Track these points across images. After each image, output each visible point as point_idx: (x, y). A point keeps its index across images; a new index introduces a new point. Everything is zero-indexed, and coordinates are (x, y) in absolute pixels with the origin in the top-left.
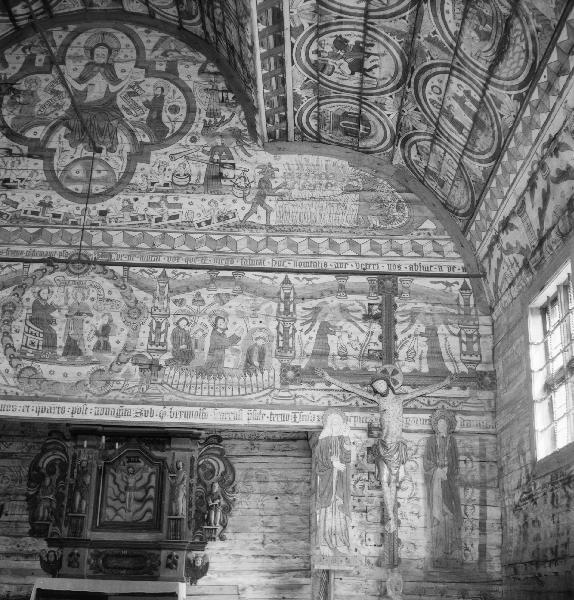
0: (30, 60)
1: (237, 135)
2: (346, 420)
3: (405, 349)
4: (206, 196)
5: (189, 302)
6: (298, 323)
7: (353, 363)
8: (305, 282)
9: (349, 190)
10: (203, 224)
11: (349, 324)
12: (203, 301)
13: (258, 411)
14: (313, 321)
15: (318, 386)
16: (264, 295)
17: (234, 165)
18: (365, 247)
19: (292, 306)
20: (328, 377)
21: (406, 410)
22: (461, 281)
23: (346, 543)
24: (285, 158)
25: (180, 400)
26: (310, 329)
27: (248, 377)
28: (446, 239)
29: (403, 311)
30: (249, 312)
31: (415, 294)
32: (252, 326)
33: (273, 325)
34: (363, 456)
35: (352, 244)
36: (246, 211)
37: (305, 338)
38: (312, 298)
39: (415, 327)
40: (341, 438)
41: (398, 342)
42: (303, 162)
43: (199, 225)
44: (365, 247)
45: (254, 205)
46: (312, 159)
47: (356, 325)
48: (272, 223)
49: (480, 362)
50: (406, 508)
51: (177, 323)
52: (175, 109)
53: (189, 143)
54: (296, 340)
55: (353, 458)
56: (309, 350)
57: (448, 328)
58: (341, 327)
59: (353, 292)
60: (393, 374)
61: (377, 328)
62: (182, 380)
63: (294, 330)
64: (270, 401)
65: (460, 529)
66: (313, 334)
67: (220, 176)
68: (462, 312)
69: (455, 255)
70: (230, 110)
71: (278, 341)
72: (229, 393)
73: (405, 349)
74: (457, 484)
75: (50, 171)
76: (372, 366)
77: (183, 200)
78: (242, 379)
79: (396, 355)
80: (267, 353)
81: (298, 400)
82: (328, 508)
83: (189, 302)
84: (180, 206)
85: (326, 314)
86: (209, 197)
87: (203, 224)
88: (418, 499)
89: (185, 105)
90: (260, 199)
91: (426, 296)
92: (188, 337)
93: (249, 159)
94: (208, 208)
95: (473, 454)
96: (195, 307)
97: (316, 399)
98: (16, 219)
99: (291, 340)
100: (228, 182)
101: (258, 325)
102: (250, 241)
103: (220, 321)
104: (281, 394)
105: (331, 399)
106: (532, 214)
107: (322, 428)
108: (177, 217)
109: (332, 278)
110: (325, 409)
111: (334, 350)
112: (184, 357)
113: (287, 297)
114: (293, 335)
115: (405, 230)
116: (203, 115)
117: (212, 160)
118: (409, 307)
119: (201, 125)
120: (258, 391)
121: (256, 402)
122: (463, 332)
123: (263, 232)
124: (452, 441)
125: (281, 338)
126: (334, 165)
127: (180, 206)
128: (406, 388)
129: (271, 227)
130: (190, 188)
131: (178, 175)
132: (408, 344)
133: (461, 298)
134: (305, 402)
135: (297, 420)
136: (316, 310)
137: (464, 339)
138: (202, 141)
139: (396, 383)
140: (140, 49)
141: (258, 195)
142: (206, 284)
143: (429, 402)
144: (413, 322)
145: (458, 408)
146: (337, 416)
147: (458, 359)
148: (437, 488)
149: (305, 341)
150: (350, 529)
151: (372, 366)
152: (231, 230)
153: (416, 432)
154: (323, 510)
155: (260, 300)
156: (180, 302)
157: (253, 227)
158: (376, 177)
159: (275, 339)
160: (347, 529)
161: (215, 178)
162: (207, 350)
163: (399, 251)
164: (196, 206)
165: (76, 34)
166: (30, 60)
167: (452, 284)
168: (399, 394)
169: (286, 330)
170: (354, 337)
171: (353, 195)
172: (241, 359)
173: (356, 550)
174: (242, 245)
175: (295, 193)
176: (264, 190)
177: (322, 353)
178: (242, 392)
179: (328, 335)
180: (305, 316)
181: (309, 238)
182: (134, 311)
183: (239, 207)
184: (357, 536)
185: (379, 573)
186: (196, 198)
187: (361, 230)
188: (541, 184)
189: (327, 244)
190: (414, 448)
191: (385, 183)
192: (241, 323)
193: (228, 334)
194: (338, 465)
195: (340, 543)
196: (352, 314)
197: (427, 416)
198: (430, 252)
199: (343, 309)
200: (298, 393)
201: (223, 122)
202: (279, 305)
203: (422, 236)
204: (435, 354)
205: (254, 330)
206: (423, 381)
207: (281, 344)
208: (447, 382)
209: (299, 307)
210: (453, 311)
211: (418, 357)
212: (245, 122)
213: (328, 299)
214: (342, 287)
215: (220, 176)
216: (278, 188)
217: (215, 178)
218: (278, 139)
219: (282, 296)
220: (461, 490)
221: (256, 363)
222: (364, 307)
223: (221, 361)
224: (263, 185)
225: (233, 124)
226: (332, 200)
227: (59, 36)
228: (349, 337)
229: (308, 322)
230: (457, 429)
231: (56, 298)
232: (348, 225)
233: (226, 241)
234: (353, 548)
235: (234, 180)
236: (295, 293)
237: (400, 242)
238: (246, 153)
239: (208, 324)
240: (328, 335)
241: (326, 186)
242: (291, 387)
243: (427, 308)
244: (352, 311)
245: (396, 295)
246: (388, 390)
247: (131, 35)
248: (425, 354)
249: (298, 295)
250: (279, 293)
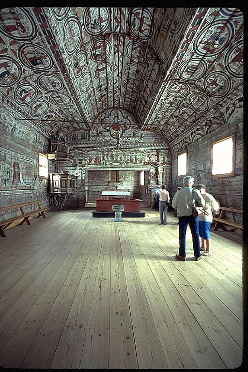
0: (106, 115)
1: (137, 128)
9: (153, 137)
31: (162, 152)
52: (128, 124)
75: (110, 134)
90: (141, 138)
98: (107, 141)
106: (181, 145)
112: (131, 161)
140: (122, 114)
149: (148, 159)
161: (134, 135)
164: (132, 139)
165: (112, 111)
166: (106, 115)
176: (141, 137)
182: (125, 155)
183: (138, 139)
188: (183, 142)
194: (152, 175)
204: (164, 160)
218: (144, 130)
227: (109, 111)
231: (113, 154)
233: (136, 145)
247: (121, 112)
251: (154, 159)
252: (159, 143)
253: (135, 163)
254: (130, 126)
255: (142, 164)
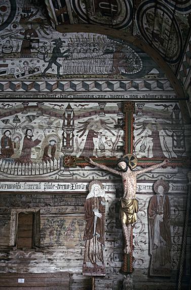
2: (103, 187)
3: (139, 145)
4: (20, 59)
5: (11, 121)
6: (76, 131)
7: (108, 154)
8: (80, 107)
9: (107, 52)
10: (20, 75)
11: (106, 130)
12: (19, 120)
13: (50, 183)
14: (85, 129)
15: (86, 168)
16: (55, 115)
17: (38, 40)
18: (116, 85)
19: (72, 122)
20: (92, 162)
21: (138, 181)
22: (174, 104)
23: (102, 260)
24: (69, 35)
25: (5, 178)
26: (82, 135)
27: (45, 164)
28: (165, 80)
29: (139, 122)
30: (45, 125)
31: (146, 113)
32: (48, 134)
33: (60, 133)
34: (113, 208)
35: (110, 85)
36: (45, 67)
37: (80, 140)
38: (84, 116)
39: (145, 131)
40: (100, 198)
41: (136, 141)
42: (80, 37)
43: (18, 76)
44: (116, 85)
45: (50, 64)
46: (86, 35)
47: (110, 131)
48: (61, 74)
49: (184, 151)
50: (138, 238)
51: (4, 133)
53: (12, 28)
54: (74, 141)
55: (107, 209)
56: (82, 146)
57: (165, 132)
58: (101, 133)
59: (109, 112)
60: (131, 160)
61: (122, 132)
62: (6, 167)
63: (73, 136)
64: (57, 178)
65: (170, 250)
66: (85, 137)
67: (31, 47)
68: (174, 122)
69: (170, 89)
70: (36, 8)
71: (63, 142)
72: (33, 173)
73: (139, 145)
74: (169, 224)
76: (119, 155)
77: (8, 62)
78: (41, 165)
79: (134, 148)
80: (57, 150)
81: (74, 176)
82: (91, 240)
83: (11, 121)
84: (7, 65)
85: (93, 125)
86: (24, 60)
87: (20, 75)
88: (145, 233)
89: (10, 5)
90: (53, 60)
91: (152, 113)
92: (10, 140)
93: (48, 36)
94: (24, 66)
95: (179, 206)
96: (15, 124)
97: (86, 175)
99: (71, 142)
100: (34, 51)
101: (51, 133)
102: (48, 85)
103: (29, 131)
104: (65, 173)
105: (94, 175)
107: (88, 192)
108: (5, 72)
109: (97, 104)
110: (89, 181)
111: (96, 146)
113: (69, 116)
114: (72, 138)
115: (139, 75)
116: (21, 11)
117: (25, 38)
118: (142, 120)
119: (19, 17)
120: (51, 172)
121: (50, 178)
122: (174, 134)
123: (55, 79)
124: (167, 199)
125: (65, 140)
126: (98, 37)
127: (7, 65)
128: (139, 168)
129: (59, 76)
130: (13, 55)
131: (6, 47)
132: (141, 142)
133: (174, 114)
134: (79, 177)
135: (74, 188)
136: (87, 123)
137: (175, 138)
138: (20, 27)
139: (133, 164)
141: (52, 57)
142: (22, 110)
143: (153, 176)
144: (144, 129)
145: (170, 179)
146: (98, 185)
147: (171, 150)
148: (157, 227)
149: (80, 141)
150: (104, 251)
151: (119, 155)
152: (37, 79)
153: (145, 194)
154: (88, 241)
155: (53, 119)
156: (6, 122)
157: (51, 76)
158: (123, 44)
159: (61, 141)
160: (102, 252)
162: (21, 148)
163: (136, 87)
167: (168, 106)
168: (134, 171)
169: (68, 135)
170: (109, 139)
171: (109, 55)
172: (41, 153)
173: (108, 264)
174: (43, 88)
175: (75, 55)
176: (56, 54)
177: (90, 147)
178: (45, 171)
179: (94, 138)
180: (79, 127)
181: (83, 81)
183: (41, 65)
184: (108, 256)
185: (120, 277)
186: (16, 61)
187: (115, 76)
189: (93, 85)
190: (143, 203)
191: (129, 47)
192: (41, 132)
193: (34, 139)
194: (97, 214)
195: (98, 260)
196: (108, 125)
197: (152, 184)
198: (155, 88)
199: (102, 122)
200: (75, 172)
201: (32, 15)
202: (64, 121)
203: (150, 78)
204: (157, 147)
205: (49, 136)
206: (149, 163)
207: (65, 144)
208: (164, 163)
209: (76, 122)
210: (168, 122)
211: (147, 149)
212: (45, 15)
213: (92, 117)
214: (102, 109)
215: (31, 47)
216: (64, 53)
217: (26, 50)
218: (64, 24)
219: (66, 115)
220: (172, 228)
221: (50, 156)
222: (115, 121)
223: (29, 155)
224: (56, 52)
225: (38, 16)
226: (97, 57)
228: (106, 138)
229: (81, 130)
230: (170, 191)
232: (106, 73)
234: (105, 263)
235: (38, 49)
236: (74, 114)
237: (138, 82)
238: (46, 33)
239: (22, 133)
240: (94, 138)
241: (93, 51)
242: (70, 169)
243: (153, 120)
244: (108, 124)
245: (134, 113)
246: (127, 168)
248: (151, 148)
249: (76, 115)
250: (65, 114)
251: (108, 140)
252: (132, 77)
253: (24, 159)
254: (11, 17)
255: (56, 163)
